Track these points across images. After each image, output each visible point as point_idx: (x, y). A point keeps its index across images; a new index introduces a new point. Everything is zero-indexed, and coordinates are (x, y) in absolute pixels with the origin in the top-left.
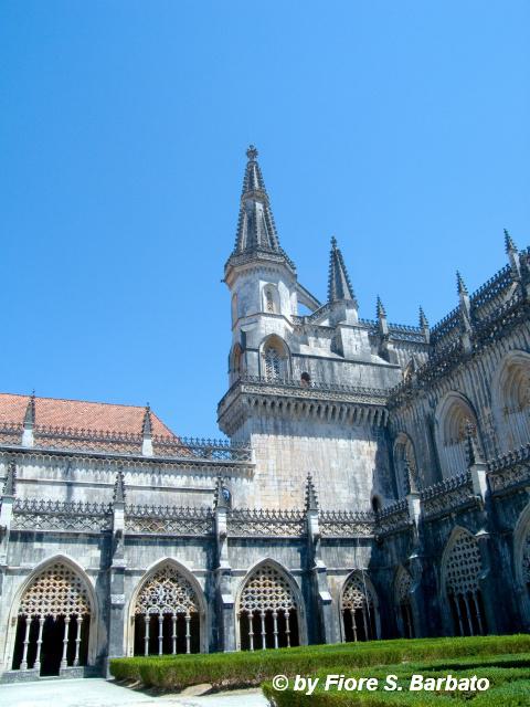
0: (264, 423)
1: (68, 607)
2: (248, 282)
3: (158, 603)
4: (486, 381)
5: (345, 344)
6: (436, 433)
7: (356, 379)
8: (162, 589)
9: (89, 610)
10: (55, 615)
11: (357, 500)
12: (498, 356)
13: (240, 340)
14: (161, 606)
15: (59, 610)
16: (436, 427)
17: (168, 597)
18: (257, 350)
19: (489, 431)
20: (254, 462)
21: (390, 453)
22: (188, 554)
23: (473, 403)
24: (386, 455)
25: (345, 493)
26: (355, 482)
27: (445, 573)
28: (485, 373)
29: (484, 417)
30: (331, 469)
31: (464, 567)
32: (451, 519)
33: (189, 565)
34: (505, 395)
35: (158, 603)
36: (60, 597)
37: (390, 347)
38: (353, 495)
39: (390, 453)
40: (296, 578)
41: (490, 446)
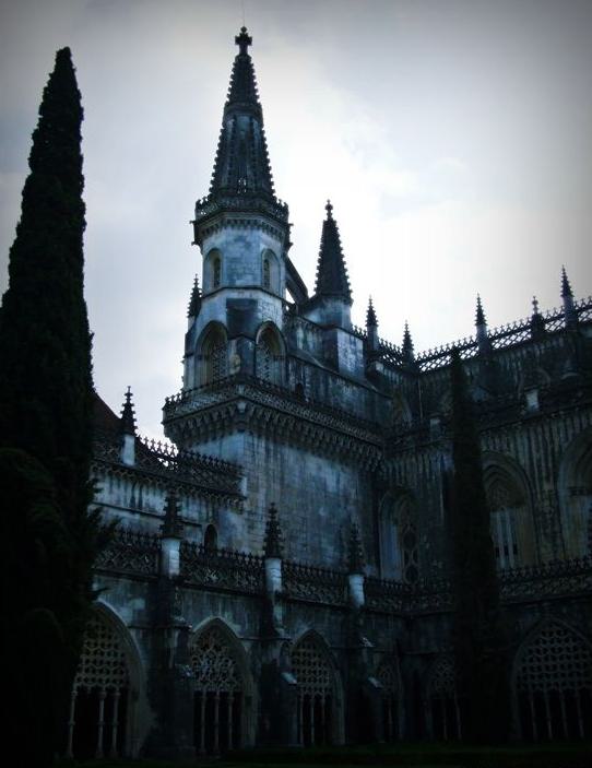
0: (256, 442)
1: (104, 677)
2: (240, 239)
3: (201, 679)
4: (553, 449)
5: (340, 355)
8: (206, 660)
9: (128, 682)
10: (90, 686)
11: (340, 561)
12: (577, 426)
13: (222, 317)
14: (204, 682)
15: (93, 680)
17: (211, 671)
18: (253, 340)
21: (375, 509)
23: (527, 468)
26: (341, 539)
28: (552, 442)
29: (542, 492)
30: (319, 517)
31: (550, 663)
33: (236, 628)
35: (201, 679)
36: (95, 662)
37: (379, 367)
38: (337, 554)
39: (375, 509)
40: (336, 655)
41: (545, 528)
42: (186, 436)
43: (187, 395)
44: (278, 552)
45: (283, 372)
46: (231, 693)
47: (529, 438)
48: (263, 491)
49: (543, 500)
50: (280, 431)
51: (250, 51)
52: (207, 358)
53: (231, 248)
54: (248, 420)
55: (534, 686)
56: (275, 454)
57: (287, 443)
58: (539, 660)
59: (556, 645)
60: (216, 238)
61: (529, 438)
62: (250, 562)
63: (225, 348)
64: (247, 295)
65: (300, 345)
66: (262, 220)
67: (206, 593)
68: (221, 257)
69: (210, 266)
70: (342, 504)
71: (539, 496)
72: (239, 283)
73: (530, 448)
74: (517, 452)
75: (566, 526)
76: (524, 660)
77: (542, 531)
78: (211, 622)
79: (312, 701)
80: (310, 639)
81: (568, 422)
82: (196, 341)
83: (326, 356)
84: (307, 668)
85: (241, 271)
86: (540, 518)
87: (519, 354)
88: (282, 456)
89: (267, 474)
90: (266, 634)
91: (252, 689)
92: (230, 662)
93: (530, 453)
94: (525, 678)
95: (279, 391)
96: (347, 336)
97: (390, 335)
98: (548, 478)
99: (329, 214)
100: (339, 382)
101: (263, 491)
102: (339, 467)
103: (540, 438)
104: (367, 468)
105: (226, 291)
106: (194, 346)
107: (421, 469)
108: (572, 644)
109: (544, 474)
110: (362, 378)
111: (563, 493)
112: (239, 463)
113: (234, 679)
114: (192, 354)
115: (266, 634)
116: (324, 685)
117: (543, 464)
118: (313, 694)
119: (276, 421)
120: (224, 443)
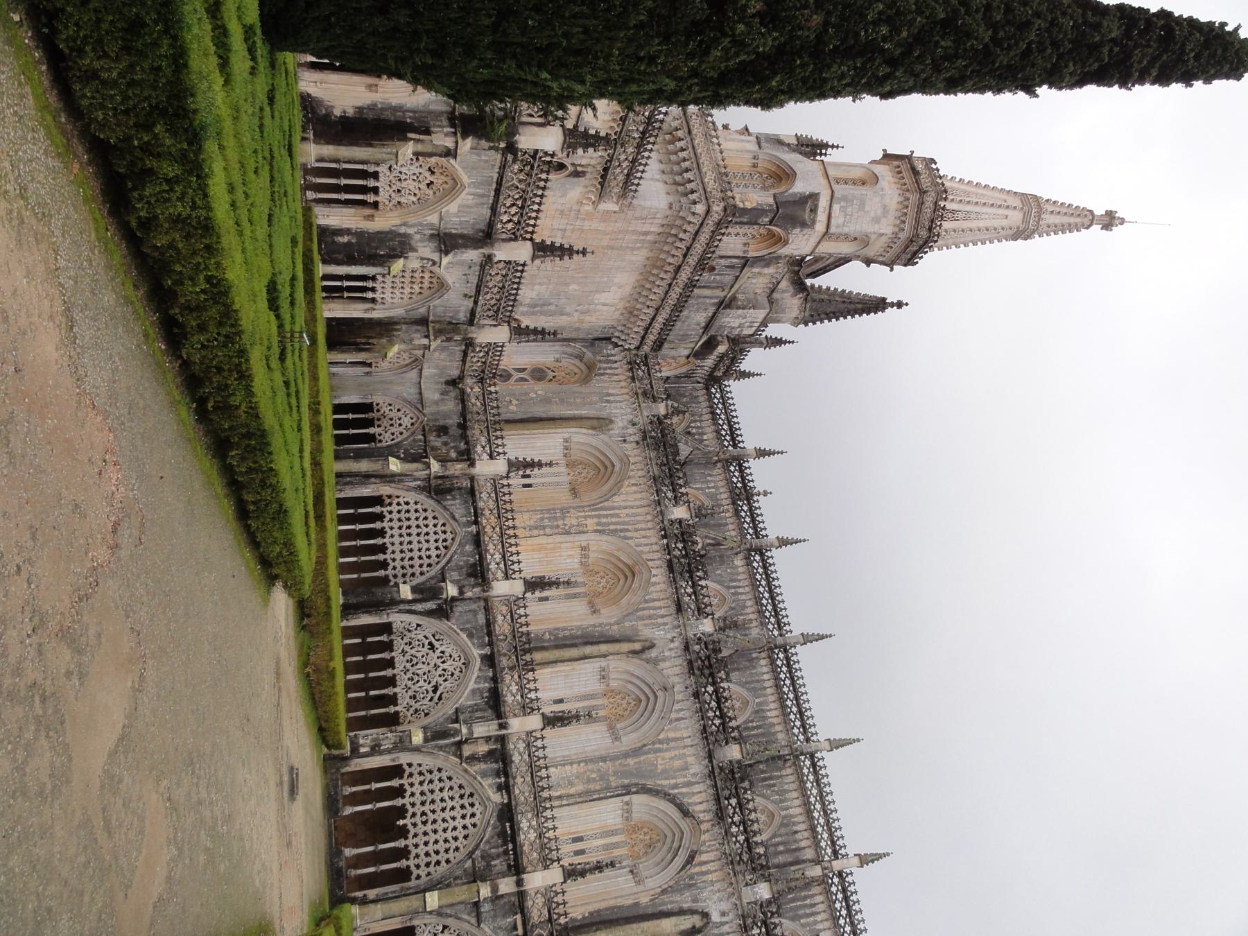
0: (656, 221)
2: (885, 209)
4: (627, 530)
6: (584, 431)
7: (687, 317)
8: (417, 171)
12: (650, 556)
13: (800, 187)
16: (591, 432)
17: (403, 177)
18: (771, 223)
19: (567, 521)
20: (603, 206)
22: (469, 207)
23: (606, 504)
24: (574, 335)
25: (534, 295)
27: (411, 497)
28: (636, 530)
29: (586, 517)
30: (568, 284)
31: (414, 531)
32: (469, 524)
33: (453, 207)
34: (602, 552)
37: (722, 349)
38: (527, 301)
41: (549, 518)
42: (668, 137)
43: (715, 140)
44: (538, 257)
45: (730, 254)
46: (377, 199)
47: (642, 506)
48: (602, 227)
50: (666, 248)
51: (1096, 228)
53: (877, 200)
54: (681, 214)
55: (390, 512)
56: (643, 241)
57: (651, 254)
58: (417, 519)
59: (432, 538)
61: (642, 506)
62: (528, 225)
63: (765, 188)
65: (756, 270)
66: (903, 236)
67: (496, 176)
68: (865, 187)
69: (857, 174)
70: (579, 308)
72: (836, 207)
73: (632, 507)
74: (627, 494)
75: (550, 539)
76: (416, 503)
78: (461, 181)
79: (370, 284)
80: (441, 286)
81: (655, 548)
82: (774, 153)
83: (740, 296)
84: (407, 280)
87: (722, 490)
88: (638, 249)
89: (620, 232)
90: (447, 242)
91: (382, 222)
92: (415, 199)
93: (625, 508)
94: (398, 504)
95: (710, 246)
96: (760, 320)
97: (753, 359)
98: (599, 524)
99: (892, 305)
100: (712, 310)
101: (602, 227)
102: (621, 306)
103: (639, 518)
104: (616, 334)
106: (770, 151)
107: (611, 391)
108: (434, 553)
109: (604, 520)
110: (712, 332)
111: (584, 537)
112: (635, 202)
113: (394, 202)
114: (760, 147)
115: (447, 242)
116: (388, 296)
117: (614, 520)
118: (378, 285)
119: (678, 244)
120: (658, 184)
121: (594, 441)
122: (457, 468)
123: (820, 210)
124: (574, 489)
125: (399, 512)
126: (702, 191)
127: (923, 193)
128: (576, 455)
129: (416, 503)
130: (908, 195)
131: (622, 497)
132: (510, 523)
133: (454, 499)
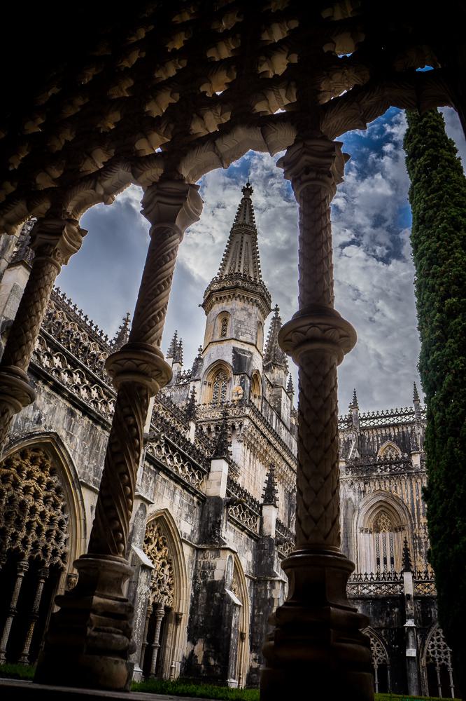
19: (422, 535)
29: (419, 523)
41: (420, 548)
49: (420, 529)
52: (210, 385)
53: (238, 313)
55: (440, 659)
60: (226, 305)
64: (246, 347)
71: (417, 525)
72: (241, 338)
73: (412, 492)
76: (432, 640)
77: (418, 550)
85: (243, 330)
86: (417, 541)
93: (412, 496)
105: (232, 341)
121: (363, 512)
122: (410, 608)
123: (242, 348)
124: (396, 530)
125: (439, 653)
126: (234, 420)
127: (237, 287)
128: (370, 525)
129: (432, 640)
130: (237, 295)
131: (405, 497)
132: (423, 575)
133: (431, 612)
